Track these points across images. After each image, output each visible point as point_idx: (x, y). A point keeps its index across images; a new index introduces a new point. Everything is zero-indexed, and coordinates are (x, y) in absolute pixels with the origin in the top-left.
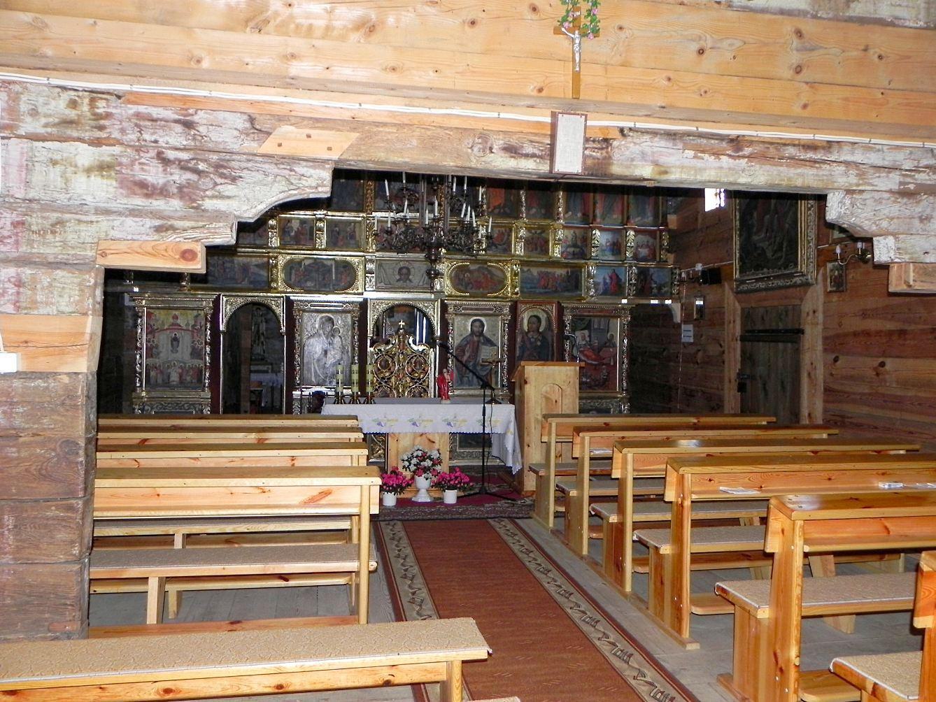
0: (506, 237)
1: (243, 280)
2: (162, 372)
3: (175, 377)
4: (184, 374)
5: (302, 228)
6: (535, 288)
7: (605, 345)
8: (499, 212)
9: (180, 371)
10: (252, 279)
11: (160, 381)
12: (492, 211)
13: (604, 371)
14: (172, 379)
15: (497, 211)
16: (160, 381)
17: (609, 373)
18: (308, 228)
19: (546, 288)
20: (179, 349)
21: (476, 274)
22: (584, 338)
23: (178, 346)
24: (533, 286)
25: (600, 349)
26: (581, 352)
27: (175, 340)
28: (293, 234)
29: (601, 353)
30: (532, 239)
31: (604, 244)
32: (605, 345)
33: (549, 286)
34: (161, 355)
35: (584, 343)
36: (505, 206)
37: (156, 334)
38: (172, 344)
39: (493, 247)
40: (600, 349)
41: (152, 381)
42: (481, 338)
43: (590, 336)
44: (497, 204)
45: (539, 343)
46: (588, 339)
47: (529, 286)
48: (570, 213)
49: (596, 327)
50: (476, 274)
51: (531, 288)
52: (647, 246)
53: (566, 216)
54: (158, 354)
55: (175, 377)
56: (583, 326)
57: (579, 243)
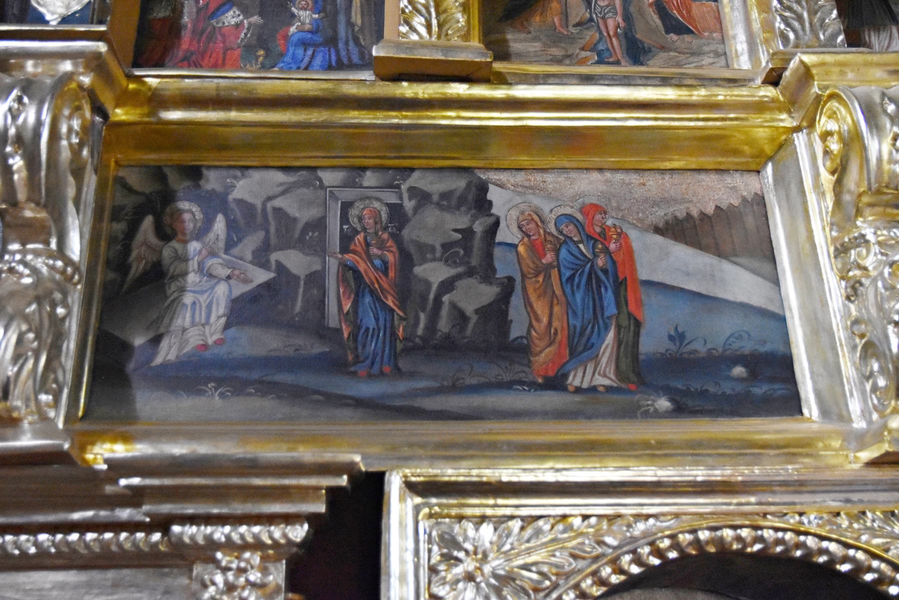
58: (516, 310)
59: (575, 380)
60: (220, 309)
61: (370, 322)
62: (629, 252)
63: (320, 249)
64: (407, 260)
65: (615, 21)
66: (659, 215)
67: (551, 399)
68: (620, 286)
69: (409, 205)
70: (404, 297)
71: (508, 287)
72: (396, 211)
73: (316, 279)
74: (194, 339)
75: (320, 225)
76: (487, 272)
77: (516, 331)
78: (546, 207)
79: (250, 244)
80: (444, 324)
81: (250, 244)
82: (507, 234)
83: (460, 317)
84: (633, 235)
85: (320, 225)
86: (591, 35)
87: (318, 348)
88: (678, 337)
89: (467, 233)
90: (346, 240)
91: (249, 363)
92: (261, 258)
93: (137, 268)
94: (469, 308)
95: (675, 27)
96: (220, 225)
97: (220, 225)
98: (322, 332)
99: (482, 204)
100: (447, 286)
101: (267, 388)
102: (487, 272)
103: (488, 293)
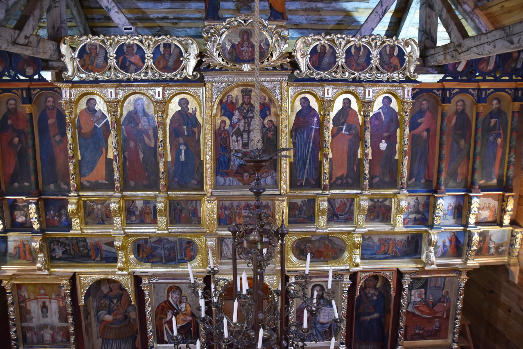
0: (348, 207)
1: (96, 257)
2: (36, 334)
3: (47, 337)
4: (56, 334)
5: (146, 207)
6: (375, 254)
7: (439, 301)
8: (342, 182)
9: (52, 332)
10: (104, 256)
11: (35, 340)
12: (335, 182)
13: (437, 324)
14: (45, 339)
15: (339, 182)
16: (35, 340)
17: (441, 325)
18: (152, 208)
19: (385, 254)
20: (49, 314)
21: (317, 244)
22: (420, 296)
23: (47, 312)
24: (373, 252)
25: (434, 305)
26: (416, 308)
27: (44, 307)
28: (137, 213)
29: (435, 308)
30: (374, 207)
31: (446, 208)
32: (439, 301)
33: (390, 252)
34: (34, 320)
35: (419, 299)
36: (347, 176)
37: (27, 303)
38: (42, 311)
39: (335, 218)
40: (434, 305)
41: (29, 340)
42: (322, 300)
43: (425, 294)
44: (339, 174)
45: (375, 298)
46: (423, 297)
47: (369, 252)
48: (414, 179)
49: (432, 285)
50: (317, 244)
51: (372, 254)
52: (489, 208)
53: (409, 183)
54: (31, 319)
55: (47, 337)
56: (419, 286)
57: (421, 209)
58: (90, 253)
59: (96, 260)
60: (61, 253)
61: (76, 254)
62: (101, 246)
63: (69, 246)
64: (79, 248)
65: (100, 217)
66: (104, 242)
67: (94, 261)
68: (100, 250)
69: (78, 241)
70: (79, 251)
71: (89, 250)
72: (77, 242)
73: (70, 250)
74: (59, 256)
75: (69, 244)
76: (87, 249)
77: (90, 255)
78: (93, 241)
79: (63, 246)
80: (83, 254)
81: (63, 246)
82: (89, 245)
83: (84, 253)
84: (102, 245)
85: (69, 244)
86: (97, 219)
87: (71, 256)
88: (106, 255)
89: (85, 245)
90: (72, 245)
91: (64, 258)
92: (64, 247)
93: (52, 249)
94: (85, 252)
95: (108, 217)
96: (59, 244)
97: (59, 244)
98: (71, 254)
99: (86, 241)
100: (83, 250)
101: (67, 260)
102: (87, 249)
103: (87, 251)
